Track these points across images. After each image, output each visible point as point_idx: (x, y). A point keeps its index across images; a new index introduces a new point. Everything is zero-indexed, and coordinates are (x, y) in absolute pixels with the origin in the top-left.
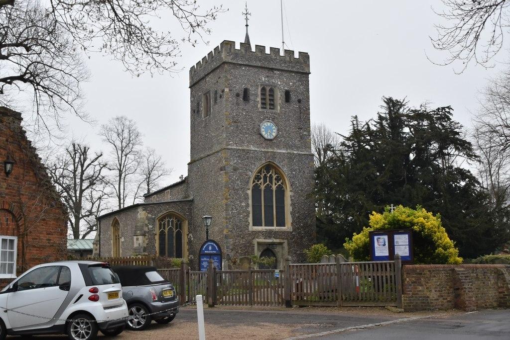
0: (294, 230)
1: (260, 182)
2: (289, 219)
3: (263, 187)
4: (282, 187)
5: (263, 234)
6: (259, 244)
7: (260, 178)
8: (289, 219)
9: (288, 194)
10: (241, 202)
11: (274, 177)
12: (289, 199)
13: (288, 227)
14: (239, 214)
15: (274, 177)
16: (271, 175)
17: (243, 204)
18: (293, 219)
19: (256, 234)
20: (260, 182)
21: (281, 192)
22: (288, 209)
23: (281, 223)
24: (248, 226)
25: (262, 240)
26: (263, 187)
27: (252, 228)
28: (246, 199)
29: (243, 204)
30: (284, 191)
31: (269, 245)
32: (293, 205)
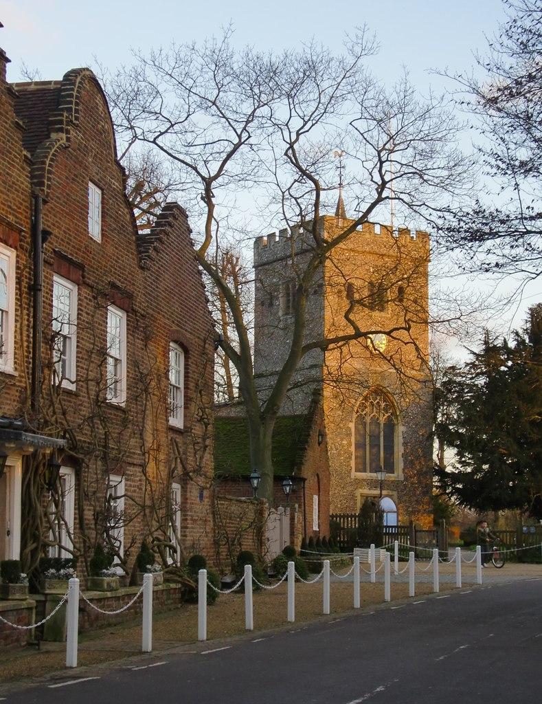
0: (406, 479)
1: (364, 412)
2: (400, 464)
3: (368, 419)
4: (392, 420)
5: (368, 484)
6: (362, 495)
7: (366, 407)
8: (400, 464)
9: (401, 429)
10: (342, 440)
11: (383, 405)
12: (401, 434)
13: (398, 474)
14: (339, 455)
15: (383, 405)
16: (378, 402)
17: (345, 442)
18: (405, 463)
19: (358, 483)
20: (364, 412)
21: (390, 428)
22: (399, 450)
23: (390, 467)
24: (350, 472)
25: (366, 491)
26: (368, 419)
27: (355, 475)
28: (349, 435)
29: (345, 442)
30: (394, 425)
31: (374, 497)
32: (405, 444)
